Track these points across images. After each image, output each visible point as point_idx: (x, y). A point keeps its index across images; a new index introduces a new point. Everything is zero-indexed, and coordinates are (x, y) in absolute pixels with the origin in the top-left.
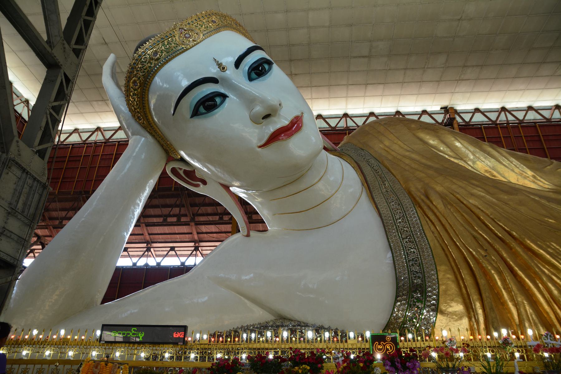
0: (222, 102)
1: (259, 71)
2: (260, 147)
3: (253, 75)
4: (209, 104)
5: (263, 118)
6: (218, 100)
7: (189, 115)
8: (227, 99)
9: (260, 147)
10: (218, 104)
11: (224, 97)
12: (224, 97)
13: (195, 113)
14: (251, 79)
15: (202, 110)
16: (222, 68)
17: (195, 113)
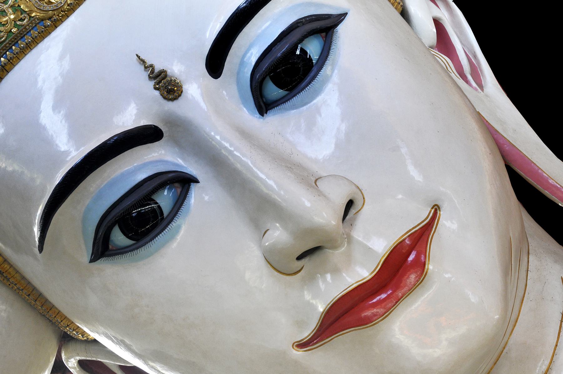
0: (180, 202)
1: (288, 73)
2: (302, 345)
3: (273, 91)
4: (138, 221)
5: (299, 258)
6: (165, 199)
7: (85, 254)
8: (194, 190)
9: (302, 345)
10: (166, 212)
11: (183, 182)
12: (183, 182)
13: (102, 249)
14: (264, 106)
15: (119, 238)
16: (169, 88)
17: (102, 249)
